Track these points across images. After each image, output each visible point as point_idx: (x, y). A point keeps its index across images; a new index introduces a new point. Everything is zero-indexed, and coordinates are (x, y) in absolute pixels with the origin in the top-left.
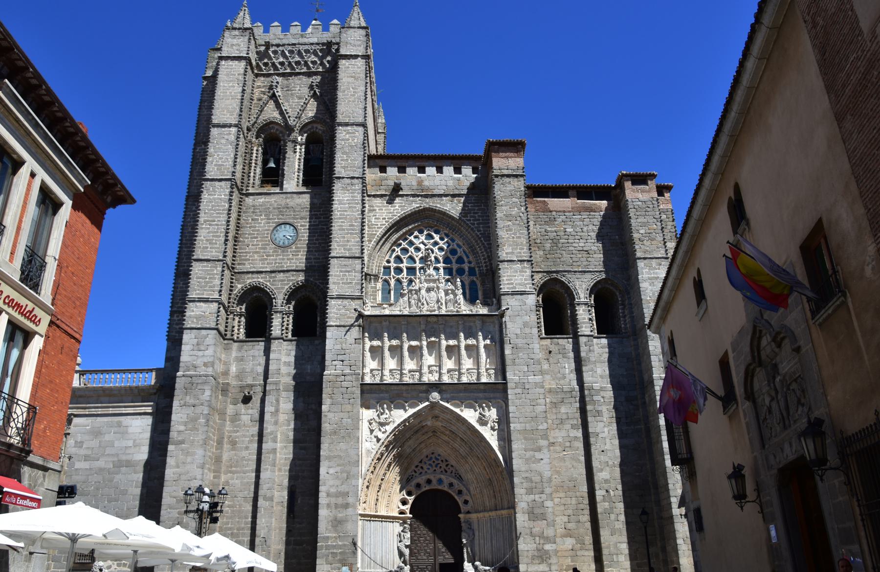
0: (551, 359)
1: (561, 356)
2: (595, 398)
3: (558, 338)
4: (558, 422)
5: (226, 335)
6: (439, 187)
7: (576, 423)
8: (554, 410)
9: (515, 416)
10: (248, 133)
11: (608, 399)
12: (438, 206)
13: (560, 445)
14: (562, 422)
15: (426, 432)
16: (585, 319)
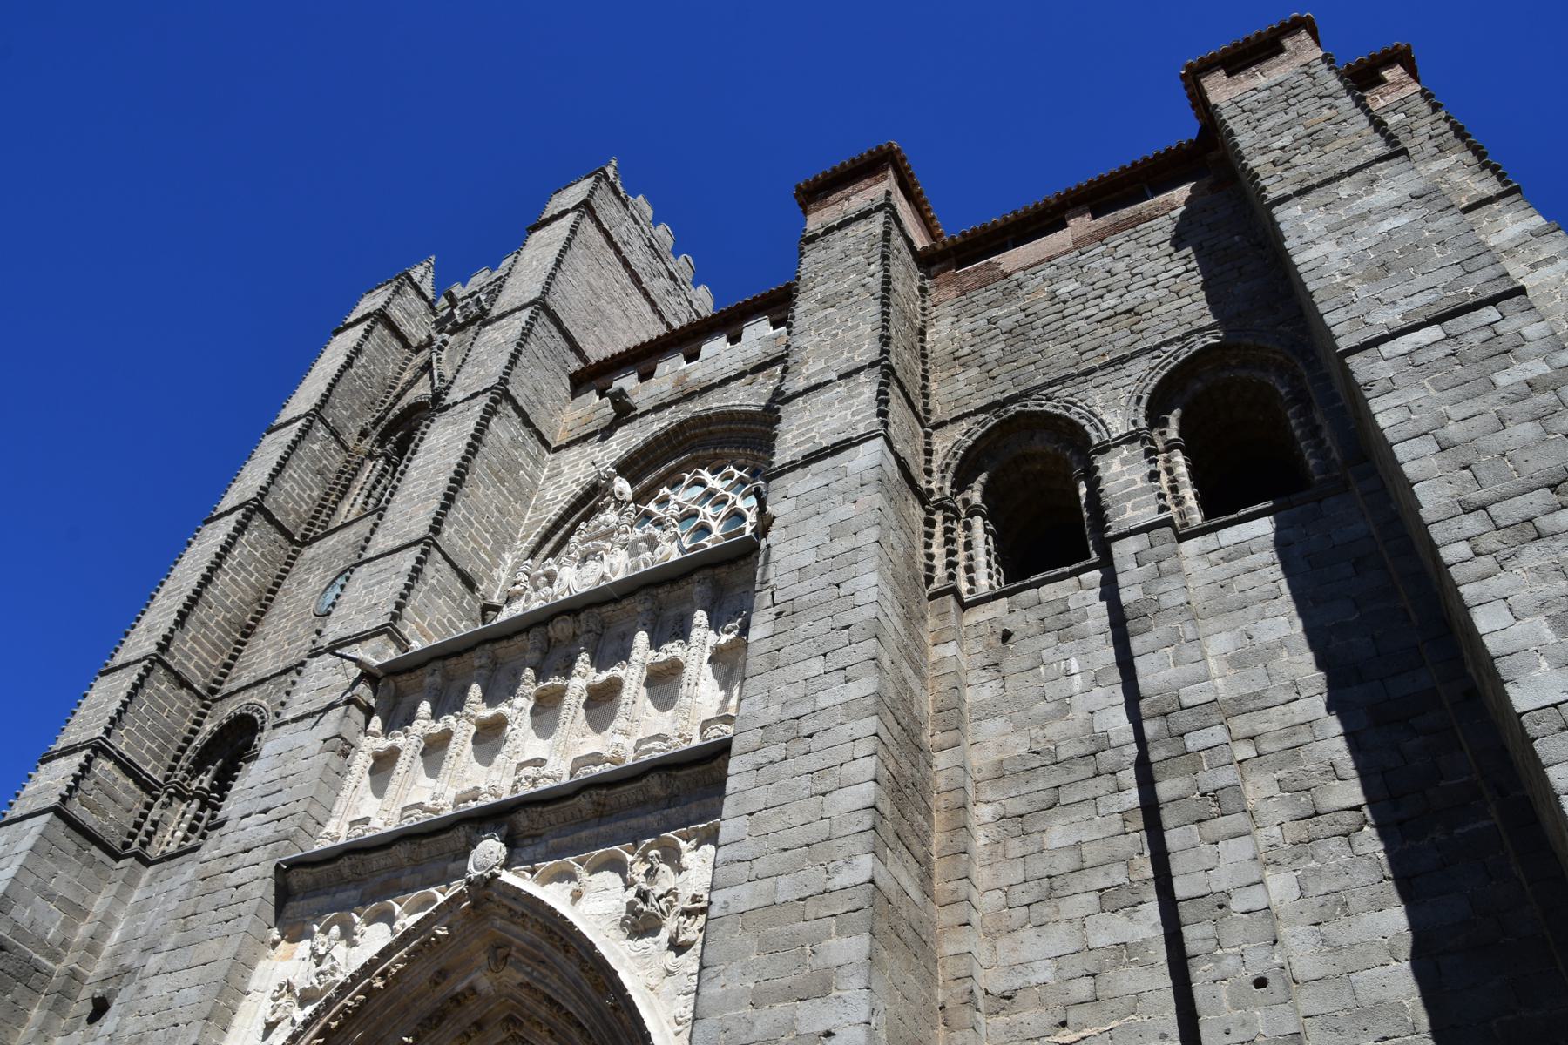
0: (1009, 665)
1: (1051, 638)
2: (1193, 742)
3: (1038, 585)
4: (1036, 891)
5: (126, 845)
6: (724, 371)
7: (1121, 880)
8: (1015, 847)
9: (737, 856)
10: (360, 441)
11: (1279, 739)
12: (715, 405)
13: (1041, 1002)
14: (1051, 889)
15: (479, 1025)
16: (1134, 482)
